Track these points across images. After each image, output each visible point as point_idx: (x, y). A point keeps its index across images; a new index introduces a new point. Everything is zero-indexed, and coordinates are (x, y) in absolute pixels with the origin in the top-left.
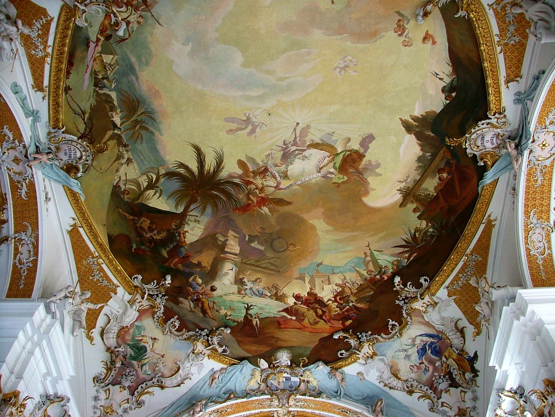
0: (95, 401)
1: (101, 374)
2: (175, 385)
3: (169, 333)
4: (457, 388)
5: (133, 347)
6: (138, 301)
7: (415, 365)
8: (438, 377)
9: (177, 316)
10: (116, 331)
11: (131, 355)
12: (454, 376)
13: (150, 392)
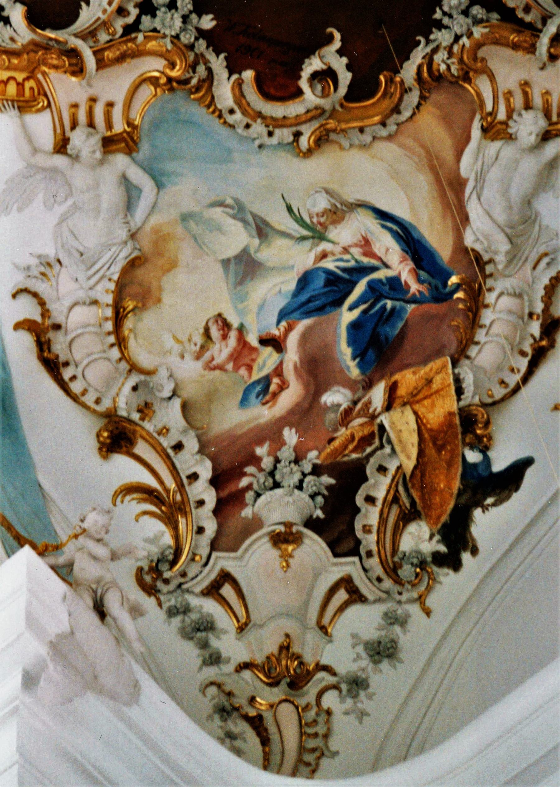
4: (336, 555)
7: (241, 330)
8: (286, 453)
12: (359, 500)
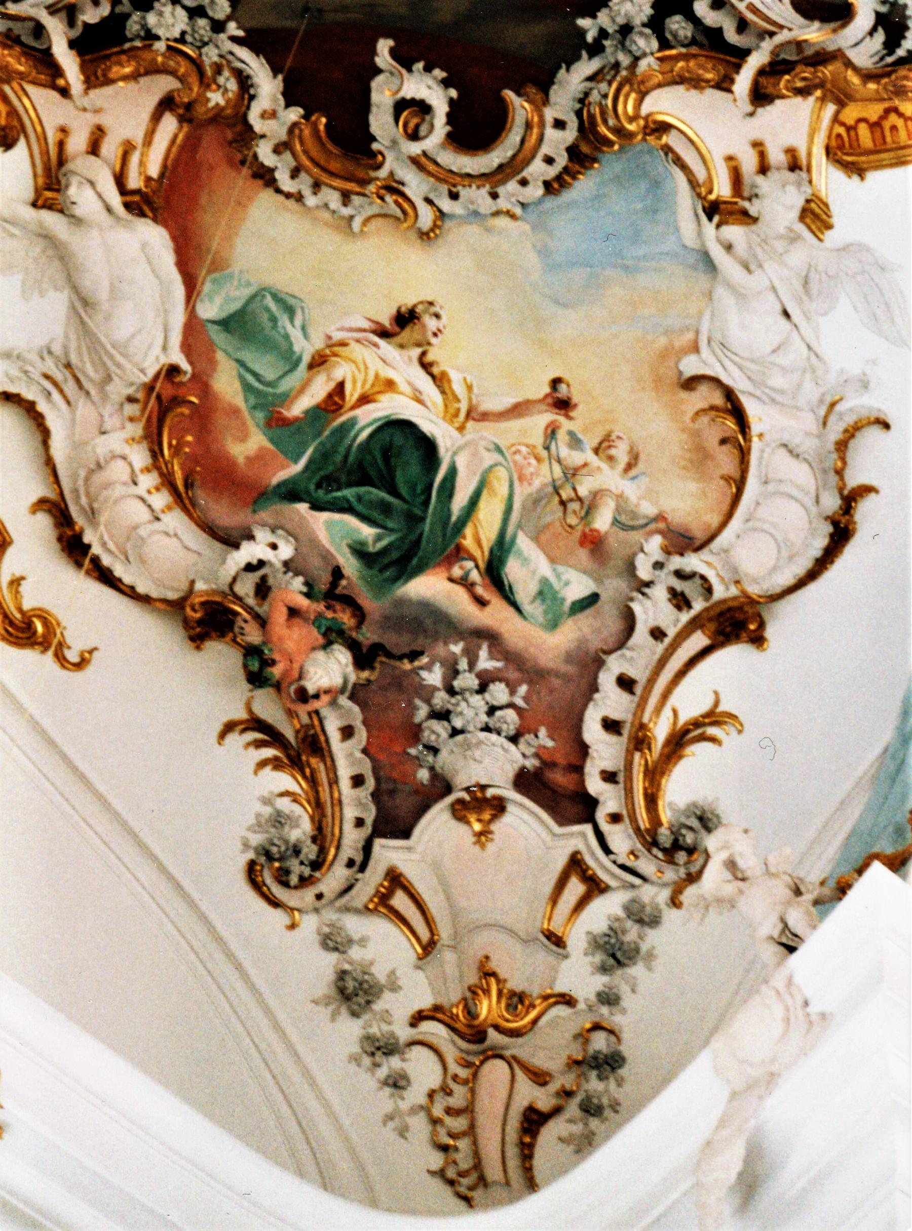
0: (355, 1014)
1: (279, 820)
2: (820, 543)
3: (446, 205)
5: (329, 482)
6: (77, 143)
9: (384, 46)
10: (140, 457)
11: (359, 551)
13: (696, 724)
